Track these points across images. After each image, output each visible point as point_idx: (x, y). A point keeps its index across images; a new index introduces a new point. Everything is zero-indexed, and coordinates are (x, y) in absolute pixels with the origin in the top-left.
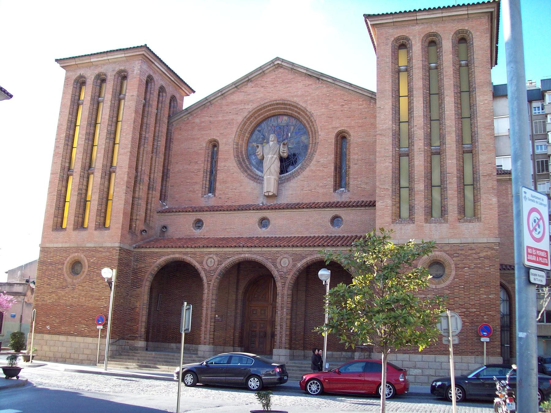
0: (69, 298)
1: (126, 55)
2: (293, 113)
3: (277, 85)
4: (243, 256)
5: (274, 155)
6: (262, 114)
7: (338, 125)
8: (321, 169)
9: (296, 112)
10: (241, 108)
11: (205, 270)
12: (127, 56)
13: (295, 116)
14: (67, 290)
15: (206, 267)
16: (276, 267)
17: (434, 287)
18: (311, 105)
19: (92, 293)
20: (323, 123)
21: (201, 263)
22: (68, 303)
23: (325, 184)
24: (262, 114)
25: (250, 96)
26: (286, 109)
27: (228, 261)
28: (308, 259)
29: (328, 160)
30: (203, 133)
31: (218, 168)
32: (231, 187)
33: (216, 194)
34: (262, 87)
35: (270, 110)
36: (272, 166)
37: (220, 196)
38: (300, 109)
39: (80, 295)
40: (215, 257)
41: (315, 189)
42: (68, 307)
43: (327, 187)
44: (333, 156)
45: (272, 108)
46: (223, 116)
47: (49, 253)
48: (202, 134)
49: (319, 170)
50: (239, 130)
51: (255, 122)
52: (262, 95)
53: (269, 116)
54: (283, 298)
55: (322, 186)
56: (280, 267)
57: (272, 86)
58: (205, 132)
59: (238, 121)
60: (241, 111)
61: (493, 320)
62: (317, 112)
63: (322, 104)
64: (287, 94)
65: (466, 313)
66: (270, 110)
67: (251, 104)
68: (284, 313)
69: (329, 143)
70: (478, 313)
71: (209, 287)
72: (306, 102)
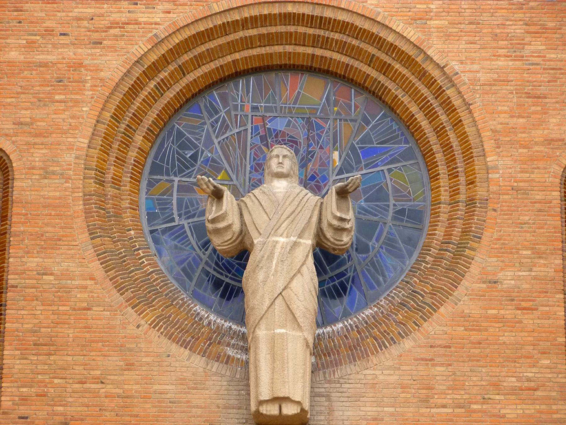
2: (357, 64)
5: (300, 236)
6: (211, 55)
8: (508, 312)
9: (371, 61)
10: (115, 17)
13: (360, 80)
18: (448, 36)
20: (503, 118)
23: (529, 380)
24: (211, 55)
26: (325, 43)
29: (535, 278)
31: (12, 279)
32: (79, 369)
35: (248, 43)
36: (296, 284)
37: (23, 410)
38: (392, 49)
41: (485, 401)
43: (539, 393)
45: (261, 37)
46: (31, 45)
49: (497, 319)
50: (107, 115)
51: (177, 88)
53: (241, 67)
55: (513, 389)
59: (102, 74)
60: (116, 31)
62: (476, 67)
63: (496, 37)
66: (248, 43)
67: (168, 6)
69: (537, 206)
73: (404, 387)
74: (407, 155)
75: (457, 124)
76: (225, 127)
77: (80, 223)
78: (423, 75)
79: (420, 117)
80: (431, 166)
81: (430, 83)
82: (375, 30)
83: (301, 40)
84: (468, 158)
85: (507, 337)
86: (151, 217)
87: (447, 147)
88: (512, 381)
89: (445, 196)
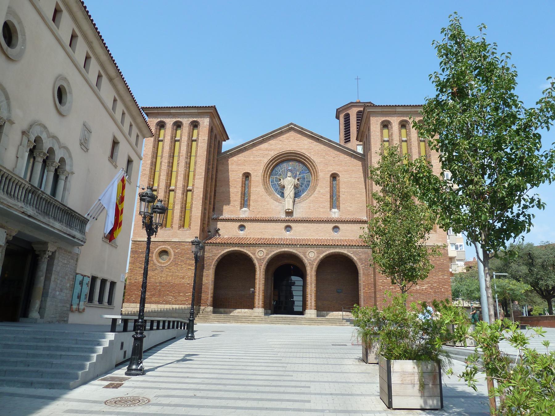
0: (158, 277)
1: (199, 111)
3: (290, 140)
7: (331, 170)
11: (257, 258)
12: (199, 112)
14: (156, 272)
15: (258, 257)
16: (306, 257)
18: (314, 155)
20: (322, 168)
21: (254, 254)
25: (272, 146)
30: (239, 167)
31: (251, 192)
33: (251, 209)
34: (281, 141)
37: (253, 210)
39: (167, 275)
42: (157, 284)
44: (329, 189)
47: (140, 245)
48: (239, 168)
49: (320, 197)
52: (280, 146)
54: (311, 277)
56: (309, 258)
58: (241, 167)
61: (447, 291)
64: (298, 147)
68: (313, 287)
70: (438, 287)
71: (260, 270)
72: (310, 153)
73: (307, 207)
74: (308, 173)
75: (315, 168)
76: (282, 169)
77: (261, 184)
78: (310, 161)
79: (310, 167)
80: (311, 174)
81: (311, 162)
83: (293, 156)
84: (317, 173)
85: (321, 200)
86: (271, 182)
87: (314, 172)
88: (322, 206)
89: (313, 179)
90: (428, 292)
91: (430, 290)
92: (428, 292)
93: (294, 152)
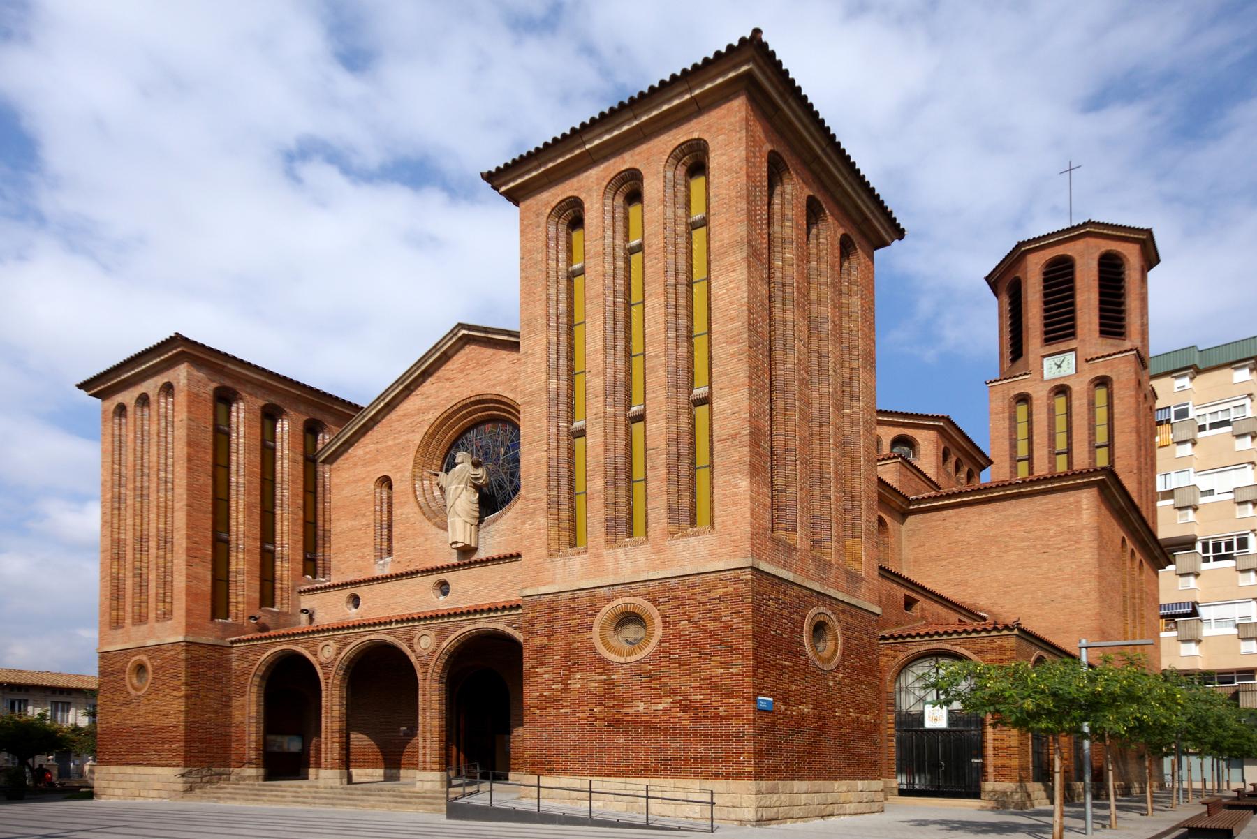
4: (367, 638)
17: (622, 660)
19: (159, 708)
22: (134, 723)
27: (349, 647)
28: (458, 633)
39: (146, 711)
40: (331, 643)
57: (461, 375)
64: (485, 384)
65: (683, 702)
82: (500, 398)
90: (672, 720)
91: (679, 715)
92: (672, 720)
93: (477, 398)
